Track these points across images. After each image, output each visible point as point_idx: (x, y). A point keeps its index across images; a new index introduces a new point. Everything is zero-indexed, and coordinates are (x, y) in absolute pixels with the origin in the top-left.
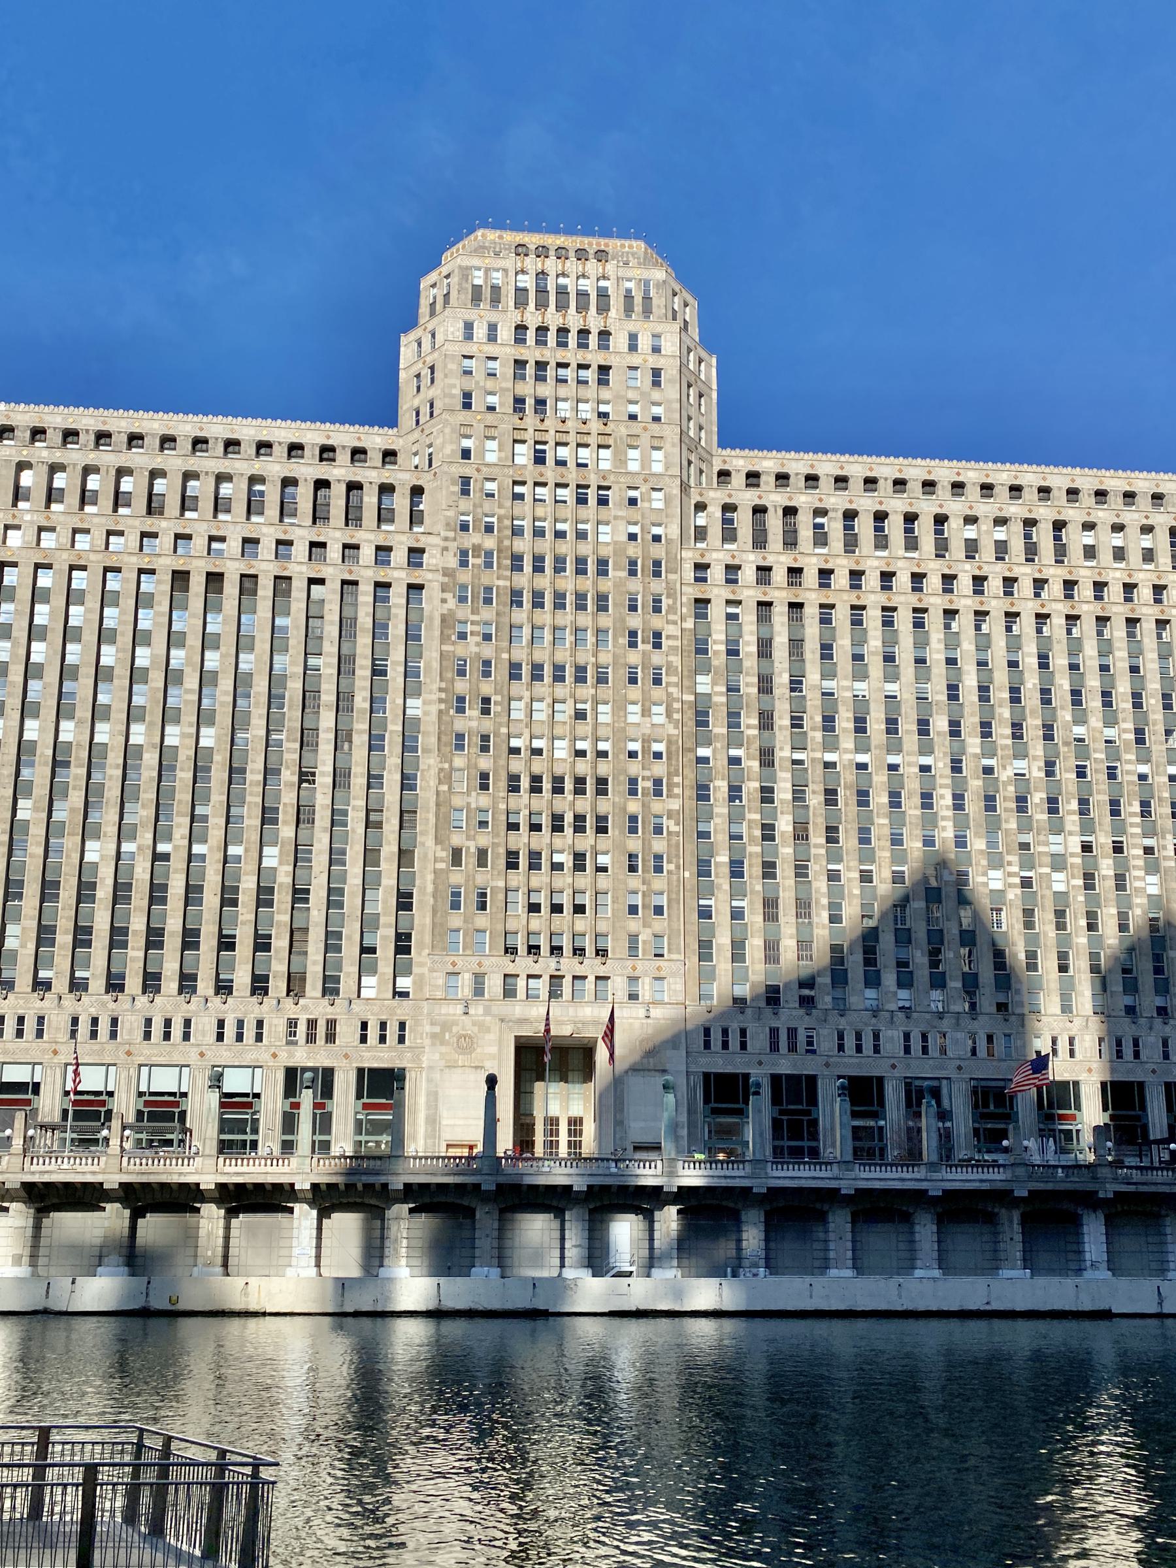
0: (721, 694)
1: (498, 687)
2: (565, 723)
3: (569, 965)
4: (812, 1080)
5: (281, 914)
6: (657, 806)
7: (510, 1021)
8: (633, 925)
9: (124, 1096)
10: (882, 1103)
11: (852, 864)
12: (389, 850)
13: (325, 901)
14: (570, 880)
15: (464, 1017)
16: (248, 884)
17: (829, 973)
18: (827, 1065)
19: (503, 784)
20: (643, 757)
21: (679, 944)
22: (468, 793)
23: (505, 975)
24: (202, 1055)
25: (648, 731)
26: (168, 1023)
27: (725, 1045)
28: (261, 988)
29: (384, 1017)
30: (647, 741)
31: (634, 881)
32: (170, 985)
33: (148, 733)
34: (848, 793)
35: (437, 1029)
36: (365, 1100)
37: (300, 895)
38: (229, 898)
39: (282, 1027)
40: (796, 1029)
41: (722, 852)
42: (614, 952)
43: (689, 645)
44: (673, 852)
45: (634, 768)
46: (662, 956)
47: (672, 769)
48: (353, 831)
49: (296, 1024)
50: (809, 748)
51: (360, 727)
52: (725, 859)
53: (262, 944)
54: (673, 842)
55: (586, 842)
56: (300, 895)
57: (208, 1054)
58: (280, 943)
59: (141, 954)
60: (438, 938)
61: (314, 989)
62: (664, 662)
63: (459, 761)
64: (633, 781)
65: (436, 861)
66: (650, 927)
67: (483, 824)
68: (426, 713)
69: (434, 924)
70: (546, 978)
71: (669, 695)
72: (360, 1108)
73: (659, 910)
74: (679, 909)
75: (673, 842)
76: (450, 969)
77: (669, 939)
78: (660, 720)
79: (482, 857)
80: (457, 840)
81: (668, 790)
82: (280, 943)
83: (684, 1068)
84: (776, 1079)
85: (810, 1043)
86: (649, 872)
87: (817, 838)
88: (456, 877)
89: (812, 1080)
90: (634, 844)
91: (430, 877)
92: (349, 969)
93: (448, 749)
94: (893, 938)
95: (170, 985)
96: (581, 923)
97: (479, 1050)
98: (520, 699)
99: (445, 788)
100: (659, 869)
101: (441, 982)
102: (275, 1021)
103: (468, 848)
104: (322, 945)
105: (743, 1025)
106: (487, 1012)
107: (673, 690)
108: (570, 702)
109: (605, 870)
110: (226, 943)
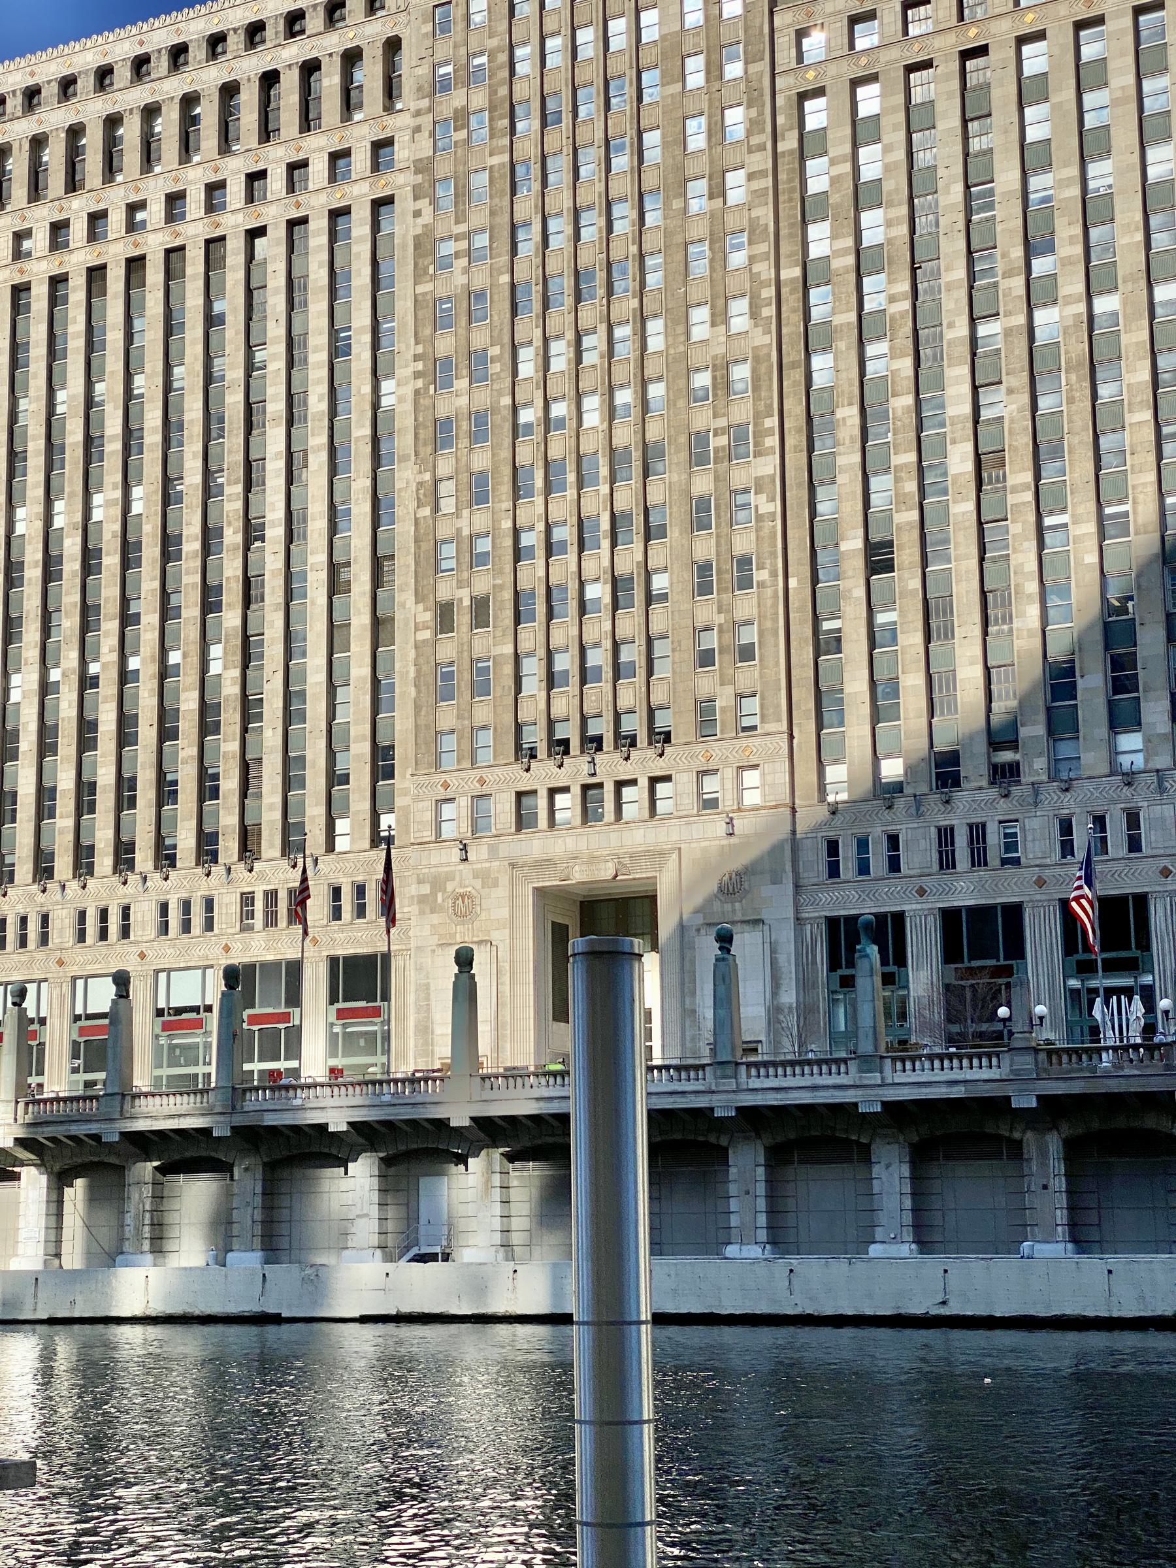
0: (842, 253)
1: (495, 334)
2: (595, 366)
3: (610, 765)
4: (1014, 913)
5: (228, 745)
6: (739, 477)
7: (524, 865)
8: (707, 683)
9: (56, 1022)
10: (1145, 944)
11: (1081, 509)
12: (360, 620)
13: (280, 714)
14: (607, 626)
15: (462, 867)
16: (189, 703)
17: (1042, 717)
18: (1040, 883)
19: (506, 488)
20: (715, 395)
21: (778, 706)
22: (457, 514)
23: (519, 795)
24: (142, 956)
25: (721, 350)
26: (104, 914)
27: (863, 868)
28: (208, 853)
29: (360, 878)
30: (722, 367)
31: (707, 611)
32: (104, 861)
33: (68, 512)
34: (1073, 377)
35: (426, 889)
36: (341, 1005)
37: (249, 709)
38: (167, 732)
39: (235, 908)
40: (984, 825)
41: (851, 533)
42: (676, 734)
43: (790, 180)
44: (766, 548)
45: (702, 419)
46: (754, 728)
47: (761, 407)
48: (313, 603)
49: (253, 898)
50: (1001, 313)
51: (316, 440)
52: (859, 544)
53: (208, 788)
54: (766, 532)
55: (629, 559)
56: (249, 709)
57: (149, 953)
58: (230, 784)
59: (70, 822)
60: (423, 749)
61: (272, 846)
62: (746, 223)
63: (445, 467)
64: (702, 438)
65: (417, 629)
66: (733, 682)
67: (480, 559)
68: (401, 400)
69: (416, 726)
70: (576, 790)
71: (754, 278)
72: (332, 1018)
73: (746, 653)
74: (777, 645)
75: (766, 532)
76: (441, 793)
77: (762, 698)
78: (740, 322)
79: (481, 609)
80: (445, 590)
81: (756, 444)
82: (230, 784)
83: (791, 914)
84: (950, 917)
85: (1011, 846)
86: (726, 589)
87: (1019, 475)
88: (447, 650)
89: (1014, 913)
90: (705, 548)
91: (412, 654)
92: (314, 814)
93: (429, 449)
94: (1162, 633)
95: (104, 861)
96: (629, 695)
97: (483, 916)
98: (529, 343)
99: (426, 511)
100: (745, 583)
101: (429, 815)
102: (226, 899)
103: (461, 600)
104: (279, 780)
105: (891, 829)
106: (493, 853)
107: (756, 268)
108: (602, 329)
109: (664, 597)
110: (166, 792)
